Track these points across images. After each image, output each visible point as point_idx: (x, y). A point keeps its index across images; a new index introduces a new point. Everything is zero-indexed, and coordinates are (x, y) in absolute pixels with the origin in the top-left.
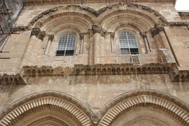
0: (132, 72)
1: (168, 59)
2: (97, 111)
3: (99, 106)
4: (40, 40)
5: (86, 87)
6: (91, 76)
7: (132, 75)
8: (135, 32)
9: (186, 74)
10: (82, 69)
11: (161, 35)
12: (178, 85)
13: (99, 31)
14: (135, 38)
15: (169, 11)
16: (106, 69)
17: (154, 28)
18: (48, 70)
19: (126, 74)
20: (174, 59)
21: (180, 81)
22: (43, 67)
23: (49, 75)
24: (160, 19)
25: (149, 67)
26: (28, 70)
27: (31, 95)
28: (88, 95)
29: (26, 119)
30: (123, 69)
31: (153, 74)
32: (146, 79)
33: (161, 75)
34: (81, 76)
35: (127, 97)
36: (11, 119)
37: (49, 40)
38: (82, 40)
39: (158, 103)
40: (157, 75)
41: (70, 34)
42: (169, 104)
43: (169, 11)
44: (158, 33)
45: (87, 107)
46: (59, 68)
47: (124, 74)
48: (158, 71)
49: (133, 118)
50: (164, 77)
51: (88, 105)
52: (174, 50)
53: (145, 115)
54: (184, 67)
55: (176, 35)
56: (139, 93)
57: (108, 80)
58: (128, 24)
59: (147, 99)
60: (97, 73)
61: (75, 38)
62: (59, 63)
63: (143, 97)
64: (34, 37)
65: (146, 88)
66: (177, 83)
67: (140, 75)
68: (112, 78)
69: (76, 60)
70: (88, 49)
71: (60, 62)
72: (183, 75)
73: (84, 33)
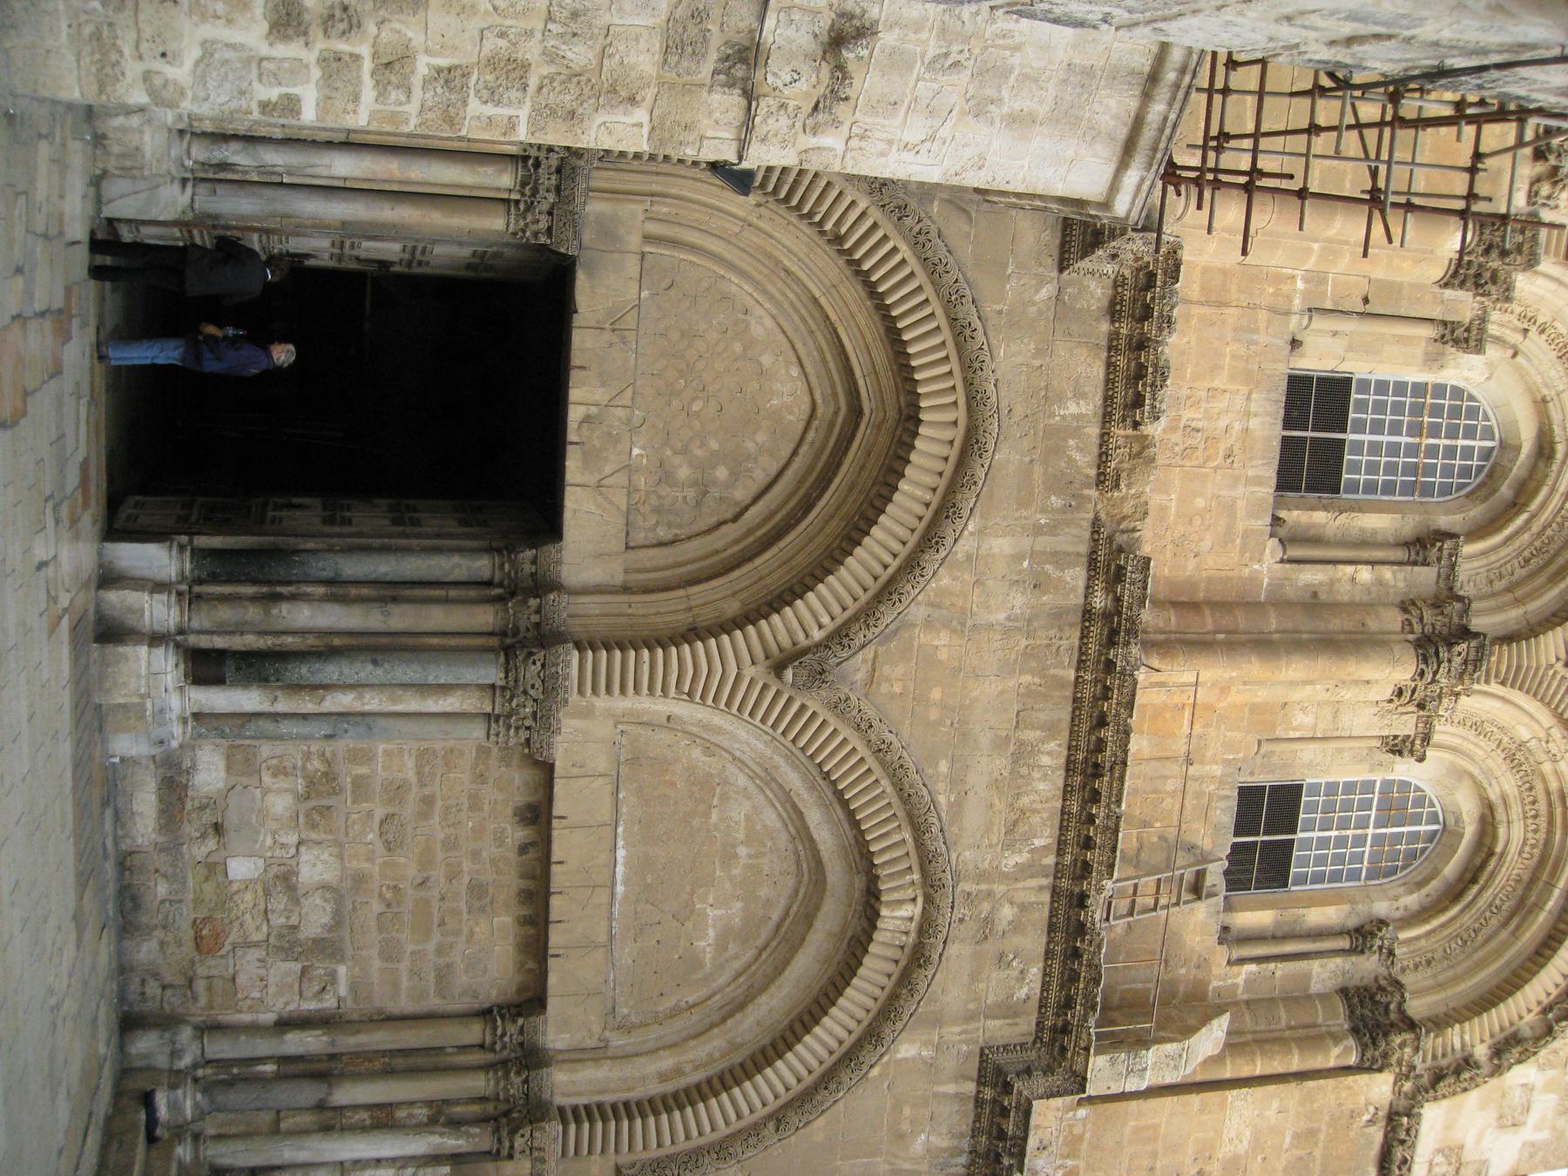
0: (1068, 859)
1: (1113, 1062)
2: (860, 676)
3: (884, 688)
5: (1008, 618)
6: (1077, 642)
7: (1050, 860)
8: (1421, 884)
9: (1010, 1128)
11: (1329, 1041)
12: (961, 1077)
13: (1429, 677)
15: (1537, 1128)
16: (1108, 733)
17: (1401, 1010)
18: (1138, 402)
20: (1109, 1092)
21: (979, 1092)
23: (1108, 399)
24: (1467, 1062)
25: (1082, 956)
26: (1151, 276)
27: (977, 324)
28: (954, 631)
29: (853, 292)
30: (1091, 819)
31: (1041, 965)
32: (1016, 926)
33: (1034, 1003)
34: (1081, 583)
36: (843, 230)
37: (1444, 323)
38: (1401, 554)
39: (875, 970)
40: (1037, 986)
41: (1487, 454)
42: (860, 1014)
43: (1537, 1128)
44: (1355, 1031)
45: (877, 631)
48: (1054, 993)
49: (815, 836)
50: (1016, 1014)
51: (898, 629)
52: (1195, 1100)
53: (828, 893)
54: (1071, 1126)
55: (1312, 1133)
56: (932, 886)
57: (1038, 733)
58: (1491, 854)
60: (1088, 677)
61: (1446, 490)
62: (1222, 424)
63: (914, 900)
65: (961, 920)
66: (975, 1074)
67: (1046, 897)
68: (1050, 753)
69: (1230, 528)
70: (1315, 594)
71: (1237, 427)
72: (1009, 1111)
73: (1453, 566)
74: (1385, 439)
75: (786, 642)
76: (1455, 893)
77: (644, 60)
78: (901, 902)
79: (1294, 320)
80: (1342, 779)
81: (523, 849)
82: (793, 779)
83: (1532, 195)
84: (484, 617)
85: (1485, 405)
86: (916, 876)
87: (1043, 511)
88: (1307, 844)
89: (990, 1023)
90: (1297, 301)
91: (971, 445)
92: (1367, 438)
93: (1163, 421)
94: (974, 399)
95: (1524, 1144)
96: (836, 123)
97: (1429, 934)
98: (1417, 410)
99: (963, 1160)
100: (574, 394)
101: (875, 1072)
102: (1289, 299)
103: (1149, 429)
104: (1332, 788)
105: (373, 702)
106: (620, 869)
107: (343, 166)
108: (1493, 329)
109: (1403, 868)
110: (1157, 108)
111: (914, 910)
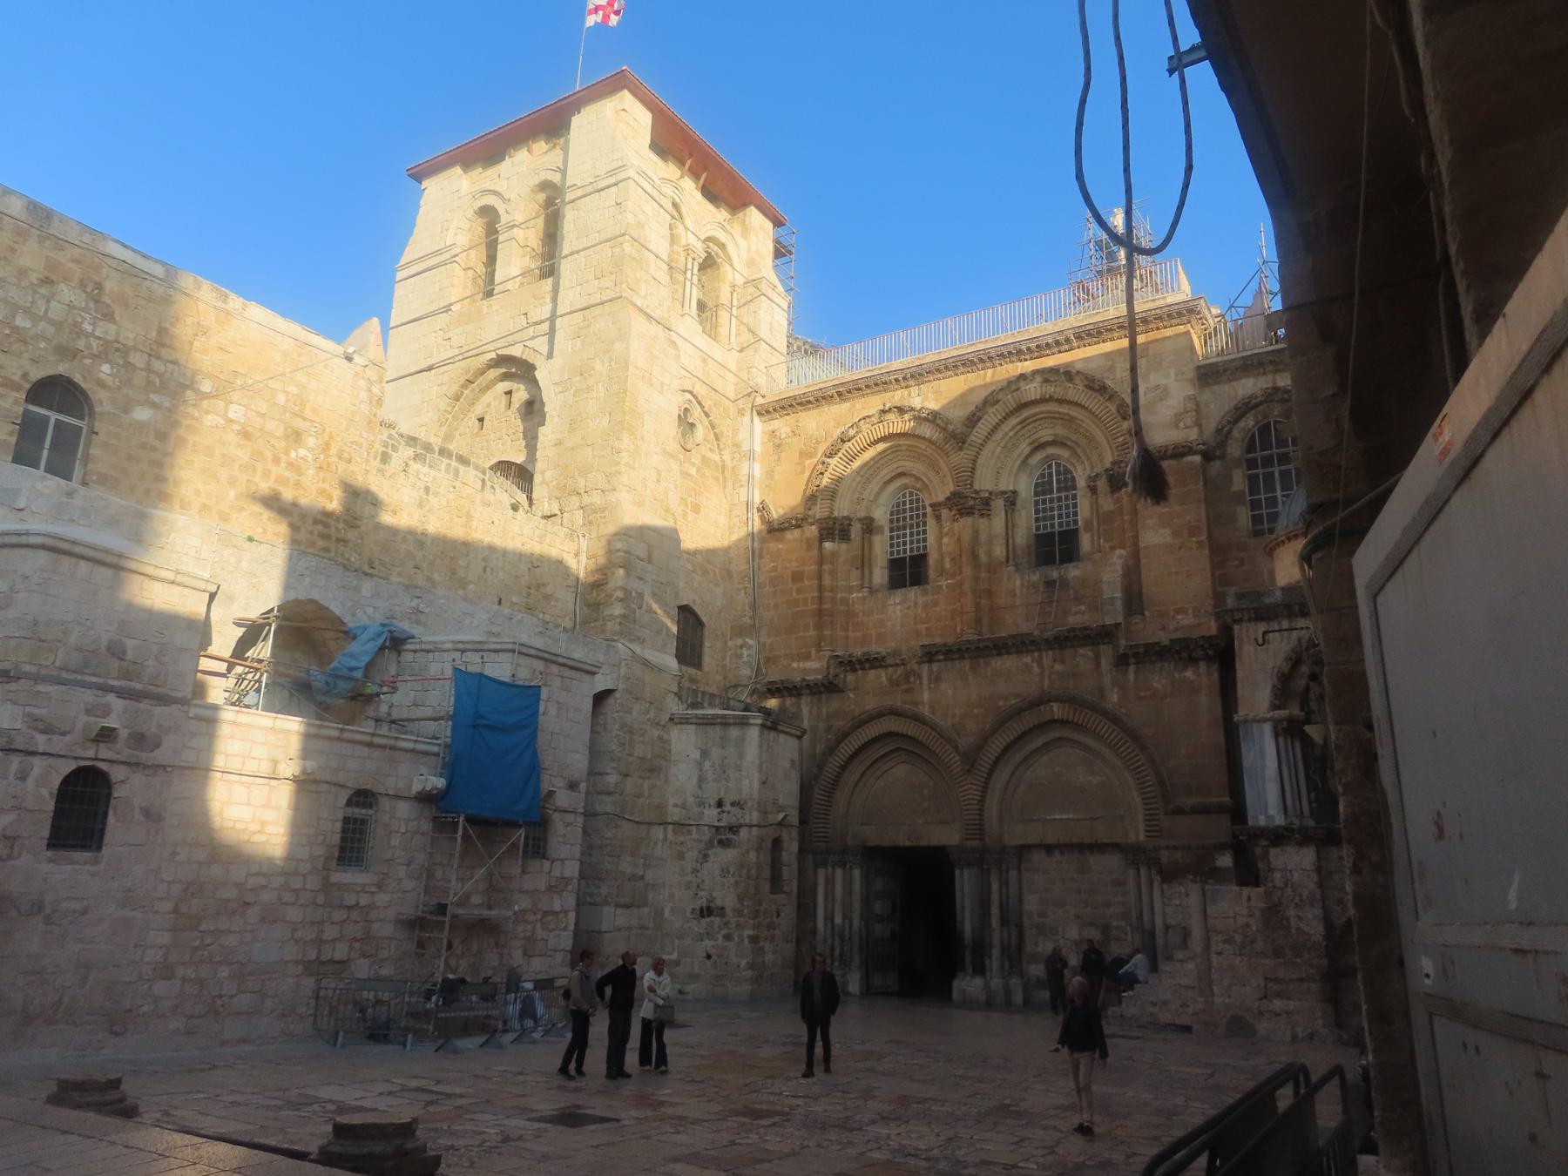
0: (1033, 648)
4: (844, 546)
7: (1036, 654)
8: (1075, 466)
9: (1141, 650)
10: (937, 652)
14: (1074, 488)
16: (981, 645)
19: (1022, 652)
22: (864, 654)
30: (1014, 644)
32: (1063, 662)
35: (1021, 711)
40: (1087, 648)
41: (911, 494)
46: (895, 653)
47: (1019, 652)
58: (1054, 441)
59: (1057, 711)
62: (898, 613)
64: (828, 545)
67: (1050, 652)
70: (953, 559)
71: (899, 607)
73: (940, 504)
74: (908, 539)
75: (958, 769)
76: (1075, 453)
77: (730, 854)
78: (1052, 711)
79: (865, 594)
80: (1034, 516)
81: (1063, 854)
82: (1018, 757)
83: (812, 524)
84: (966, 872)
85: (895, 501)
86: (1042, 707)
87: (915, 683)
88: (1060, 524)
89: (1104, 662)
90: (860, 595)
91: (895, 713)
92: (908, 547)
93: (879, 650)
94: (880, 715)
95: (1176, 380)
96: (746, 803)
97: (1089, 458)
98: (898, 529)
99: (1167, 664)
100: (901, 844)
101: (1123, 710)
102: (858, 598)
103: (884, 654)
104: (1037, 520)
105: (995, 910)
106: (1064, 817)
107: (838, 920)
108: (862, 514)
109: (1071, 472)
110: (732, 721)
111: (1055, 706)
